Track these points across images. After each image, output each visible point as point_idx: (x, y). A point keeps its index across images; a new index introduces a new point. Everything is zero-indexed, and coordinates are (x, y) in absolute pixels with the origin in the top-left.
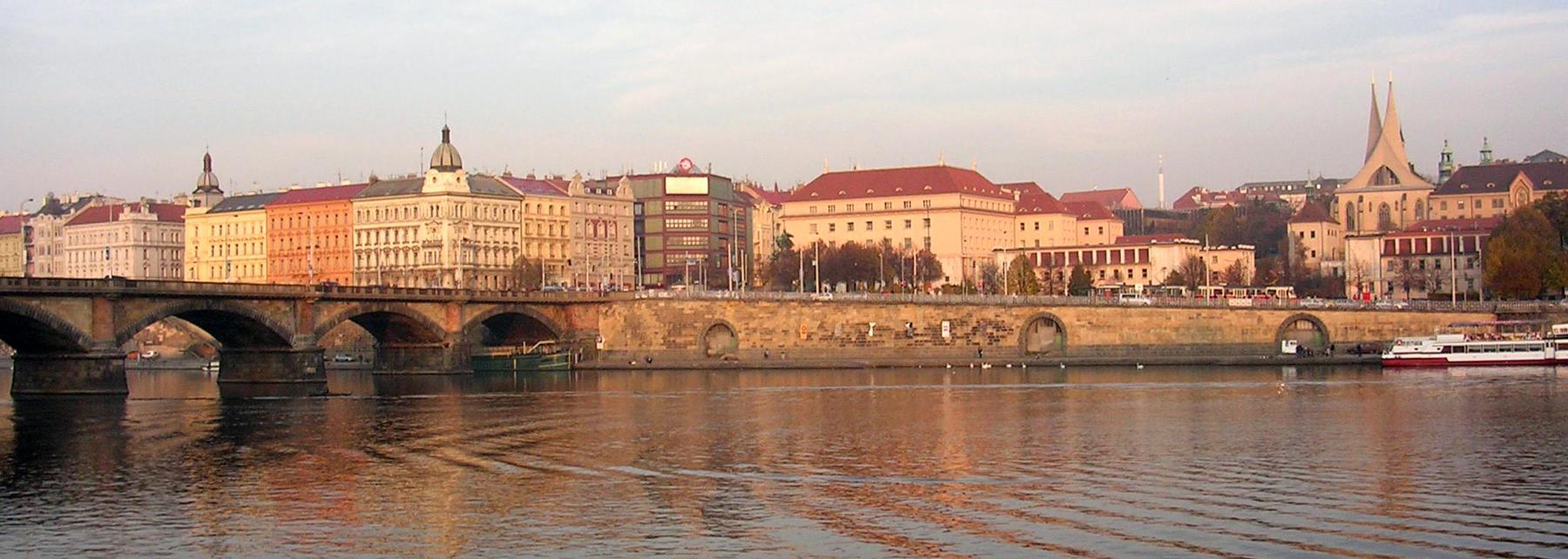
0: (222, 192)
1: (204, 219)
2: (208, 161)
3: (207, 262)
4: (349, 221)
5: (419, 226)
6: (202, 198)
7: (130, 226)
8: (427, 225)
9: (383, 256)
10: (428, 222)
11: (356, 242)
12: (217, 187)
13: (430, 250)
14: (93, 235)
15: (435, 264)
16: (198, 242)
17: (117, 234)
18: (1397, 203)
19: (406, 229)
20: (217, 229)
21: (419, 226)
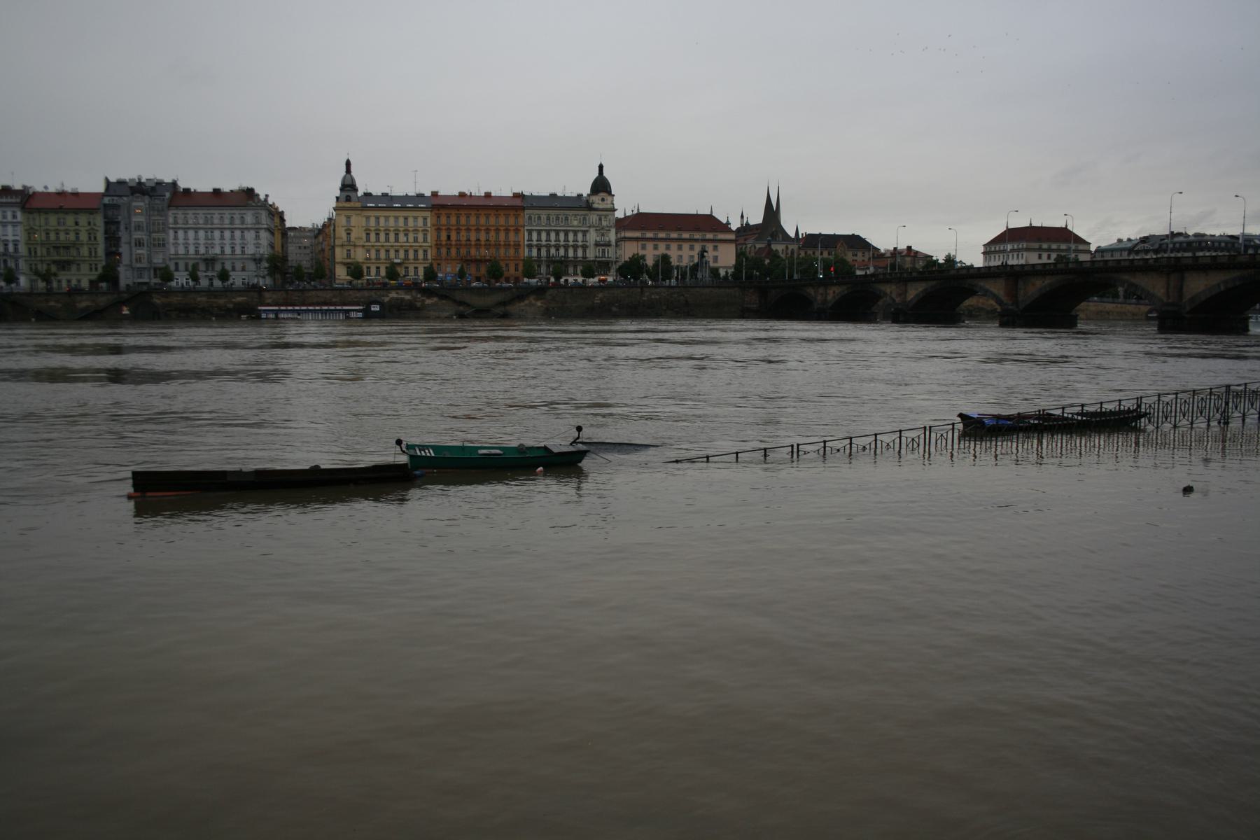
1: (358, 212)
2: (348, 164)
3: (363, 246)
4: (521, 221)
5: (587, 231)
8: (596, 230)
9: (553, 251)
10: (598, 228)
11: (526, 238)
13: (603, 248)
14: (209, 216)
15: (608, 258)
16: (351, 230)
18: (783, 250)
19: (575, 233)
20: (373, 221)
21: (587, 231)
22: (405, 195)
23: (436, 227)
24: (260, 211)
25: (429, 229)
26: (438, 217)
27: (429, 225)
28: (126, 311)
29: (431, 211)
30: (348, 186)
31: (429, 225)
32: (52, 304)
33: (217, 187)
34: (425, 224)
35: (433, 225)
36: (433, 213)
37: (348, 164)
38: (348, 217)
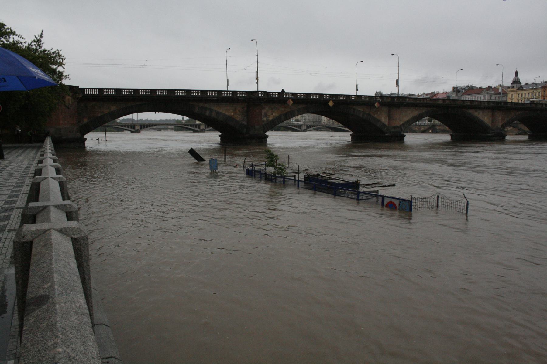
0: (521, 83)
1: (515, 92)
6: (515, 85)
7: (486, 95)
12: (519, 81)
14: (472, 98)
17: (481, 97)
20: (520, 95)
22: (541, 82)
23: (543, 96)
24: (485, 95)
25: (541, 97)
26: (544, 91)
27: (541, 95)
28: (430, 131)
29: (542, 89)
30: (516, 82)
31: (541, 95)
32: (416, 129)
33: (489, 85)
34: (539, 95)
35: (542, 95)
36: (542, 90)
37: (516, 73)
38: (512, 95)
